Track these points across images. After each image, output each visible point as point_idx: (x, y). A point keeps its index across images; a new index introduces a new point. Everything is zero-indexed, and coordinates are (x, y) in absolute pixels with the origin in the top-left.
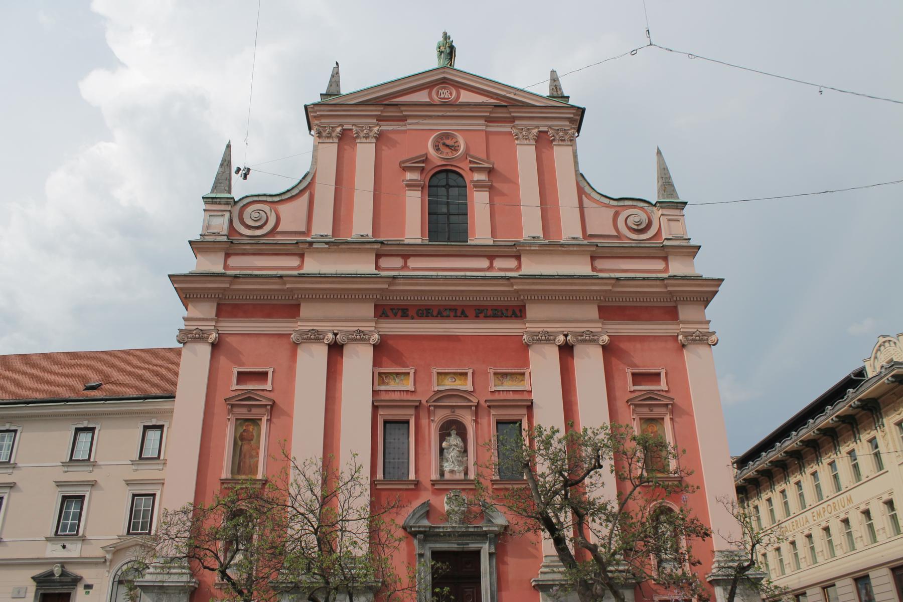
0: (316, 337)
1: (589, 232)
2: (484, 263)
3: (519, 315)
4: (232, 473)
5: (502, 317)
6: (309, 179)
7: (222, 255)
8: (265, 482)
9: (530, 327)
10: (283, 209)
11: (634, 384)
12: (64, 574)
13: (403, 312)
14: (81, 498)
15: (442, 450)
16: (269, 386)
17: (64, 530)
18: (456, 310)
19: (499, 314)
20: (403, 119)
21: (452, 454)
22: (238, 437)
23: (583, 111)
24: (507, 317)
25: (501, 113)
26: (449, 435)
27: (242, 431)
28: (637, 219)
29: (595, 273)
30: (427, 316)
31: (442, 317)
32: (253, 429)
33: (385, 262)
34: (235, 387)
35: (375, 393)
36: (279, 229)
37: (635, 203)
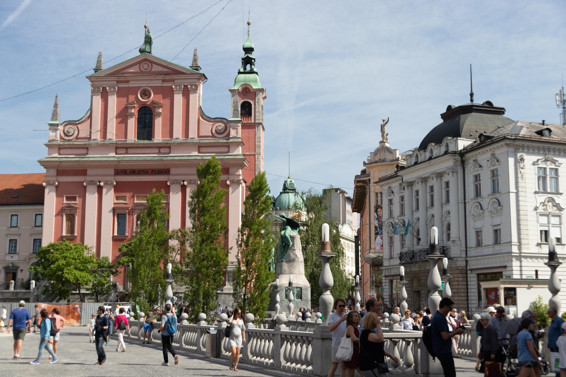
0: (92, 183)
1: (200, 135)
2: (157, 150)
4: (66, 233)
6: (89, 113)
7: (57, 149)
8: (76, 237)
9: (172, 178)
10: (78, 126)
12: (13, 267)
13: (124, 172)
14: (16, 240)
15: (137, 224)
17: (11, 251)
20: (127, 82)
23: (204, 75)
25: (168, 77)
33: (118, 151)
35: (114, 204)
36: (79, 136)
37: (221, 120)
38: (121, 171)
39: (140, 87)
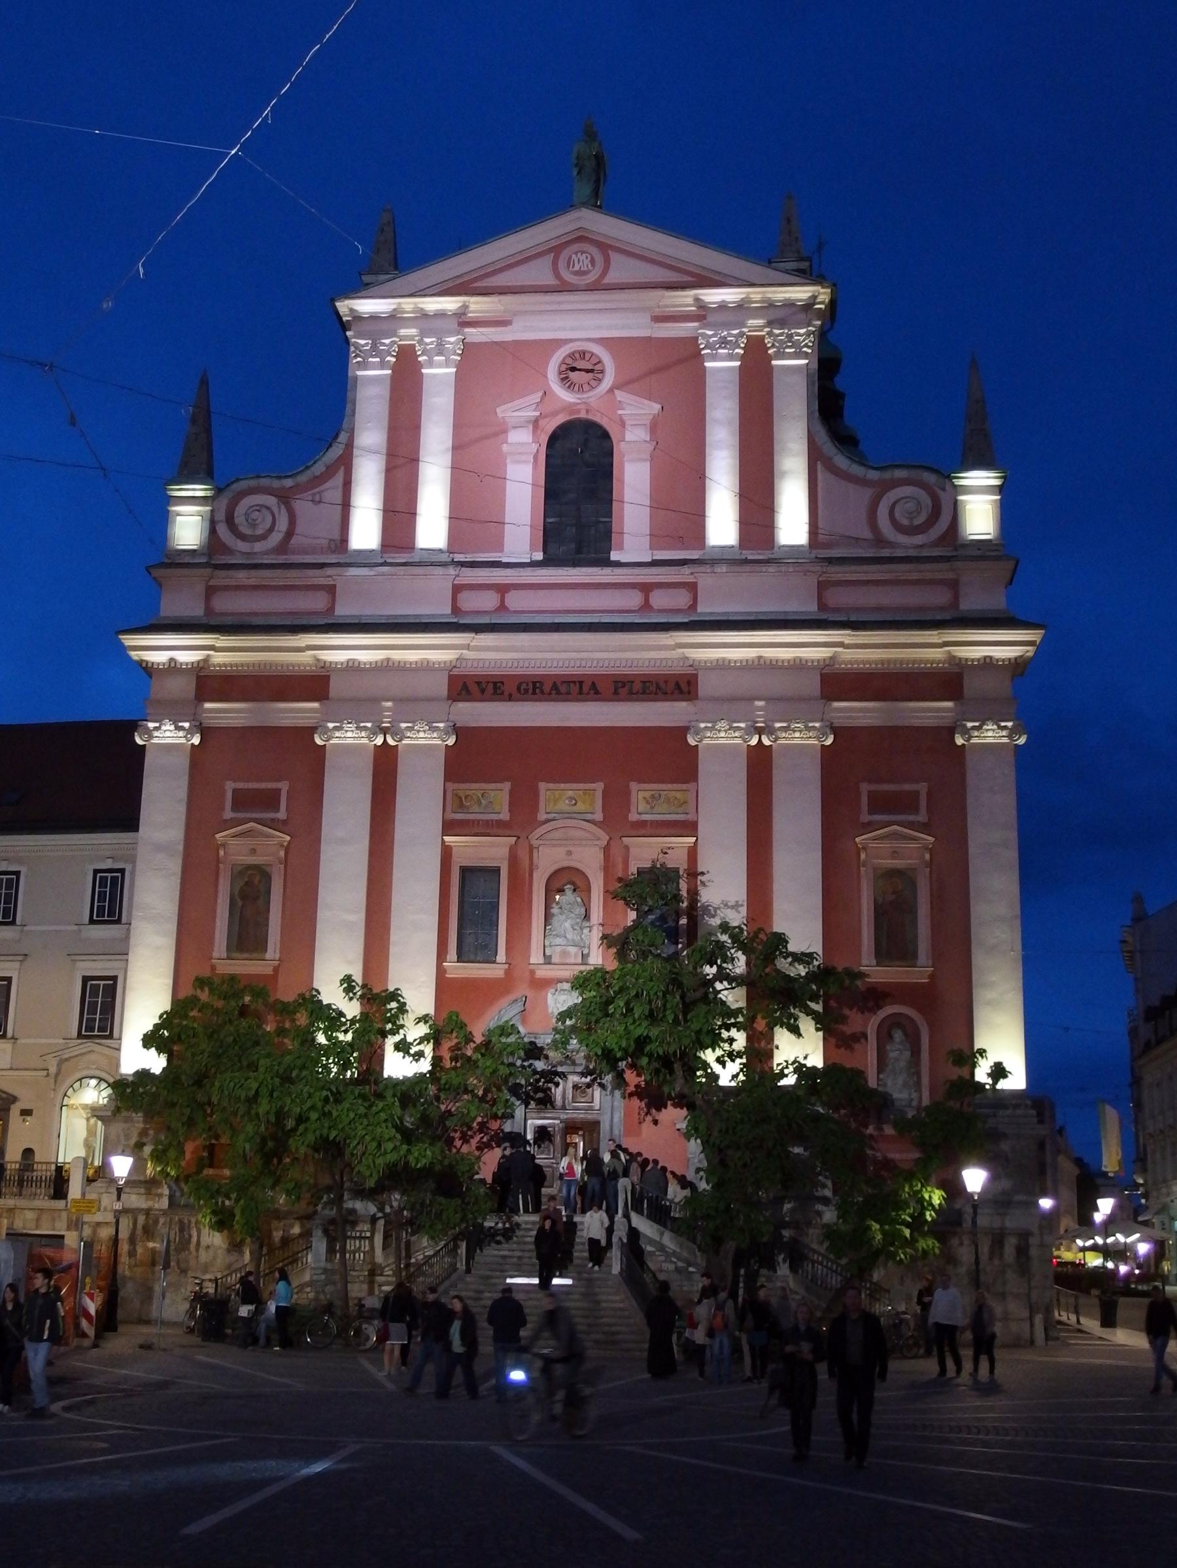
3: (684, 687)
4: (229, 949)
5: (656, 693)
11: (871, 812)
15: (548, 918)
16: (282, 815)
18: (581, 683)
19: (653, 688)
21: (565, 923)
22: (236, 893)
24: (666, 693)
26: (561, 891)
27: (242, 884)
28: (911, 506)
29: (823, 616)
30: (534, 693)
31: (559, 693)
32: (260, 882)
34: (228, 814)
38: (478, 683)
39: (558, 343)
